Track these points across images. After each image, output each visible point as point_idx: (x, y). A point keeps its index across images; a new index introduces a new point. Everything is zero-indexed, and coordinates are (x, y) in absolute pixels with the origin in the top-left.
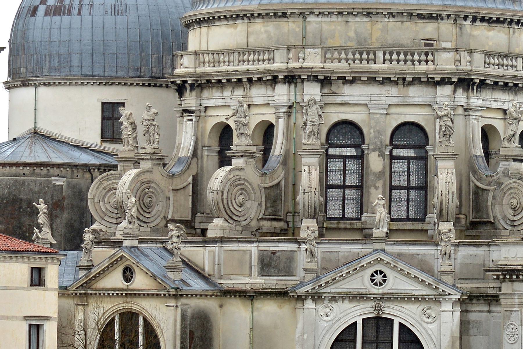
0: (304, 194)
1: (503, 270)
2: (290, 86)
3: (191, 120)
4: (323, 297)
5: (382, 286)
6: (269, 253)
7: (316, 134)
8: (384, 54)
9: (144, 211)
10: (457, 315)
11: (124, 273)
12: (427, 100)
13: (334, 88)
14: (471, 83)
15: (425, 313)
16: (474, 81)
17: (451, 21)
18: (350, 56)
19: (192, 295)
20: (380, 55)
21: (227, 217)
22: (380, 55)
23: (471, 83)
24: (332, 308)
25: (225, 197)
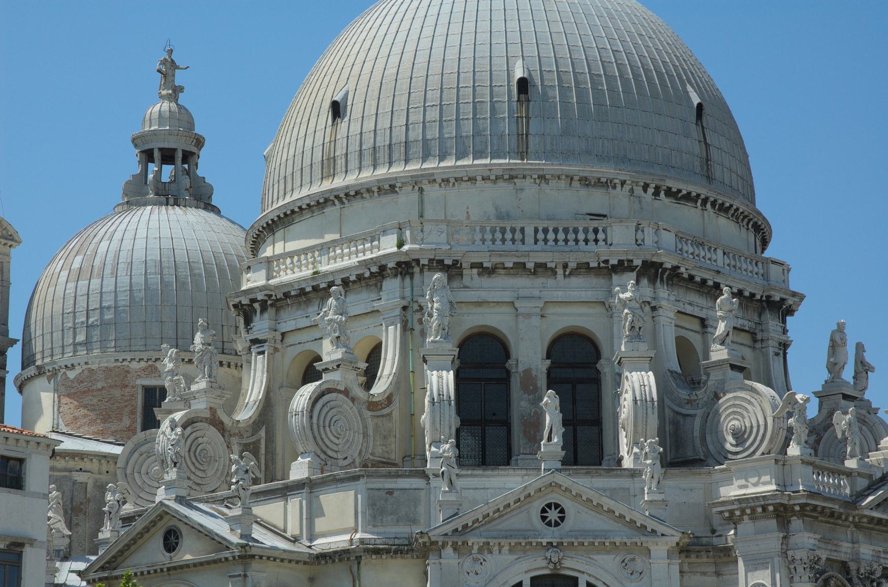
0: (433, 405)
1: (740, 501)
2: (403, 279)
3: (263, 353)
4: (470, 544)
5: (559, 527)
6: (383, 493)
7: (446, 328)
8: (536, 231)
9: (196, 468)
10: (676, 568)
11: (166, 538)
12: (599, 295)
13: (466, 280)
14: (660, 270)
15: (626, 567)
16: (664, 266)
17: (627, 187)
18: (488, 236)
19: (268, 558)
20: (530, 231)
21: (319, 452)
22: (530, 231)
23: (660, 270)
24: (484, 560)
25: (315, 420)
